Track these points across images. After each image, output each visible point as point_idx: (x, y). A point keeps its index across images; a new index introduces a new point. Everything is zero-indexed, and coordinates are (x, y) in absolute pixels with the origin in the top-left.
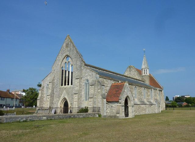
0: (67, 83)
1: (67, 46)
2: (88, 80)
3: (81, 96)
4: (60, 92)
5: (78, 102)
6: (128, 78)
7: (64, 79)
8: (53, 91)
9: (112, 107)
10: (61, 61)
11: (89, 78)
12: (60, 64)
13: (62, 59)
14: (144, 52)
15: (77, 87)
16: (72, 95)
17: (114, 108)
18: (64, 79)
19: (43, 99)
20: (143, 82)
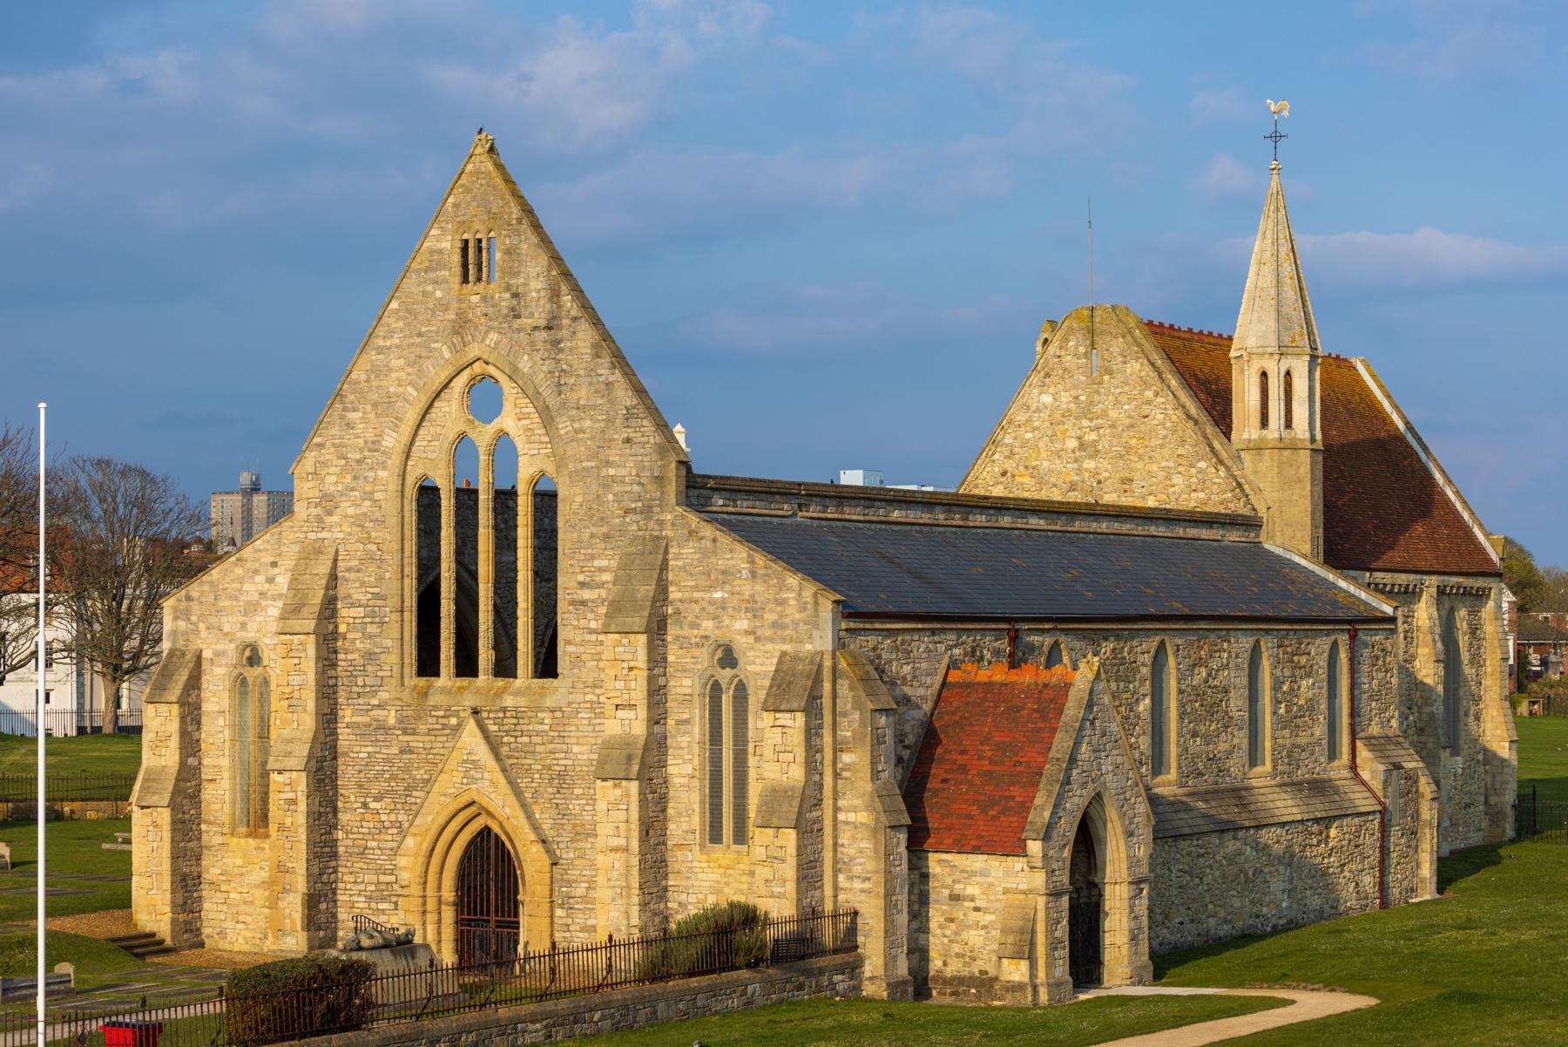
0: (486, 656)
1: (472, 260)
2: (728, 658)
3: (662, 801)
4: (416, 742)
5: (643, 854)
6: (1078, 525)
7: (447, 607)
8: (328, 719)
9: (955, 898)
10: (412, 416)
11: (747, 633)
12: (392, 441)
13: (416, 399)
14: (1276, 137)
15: (630, 714)
16: (561, 780)
17: (973, 916)
18: (447, 607)
19: (195, 798)
20: (1234, 536)
